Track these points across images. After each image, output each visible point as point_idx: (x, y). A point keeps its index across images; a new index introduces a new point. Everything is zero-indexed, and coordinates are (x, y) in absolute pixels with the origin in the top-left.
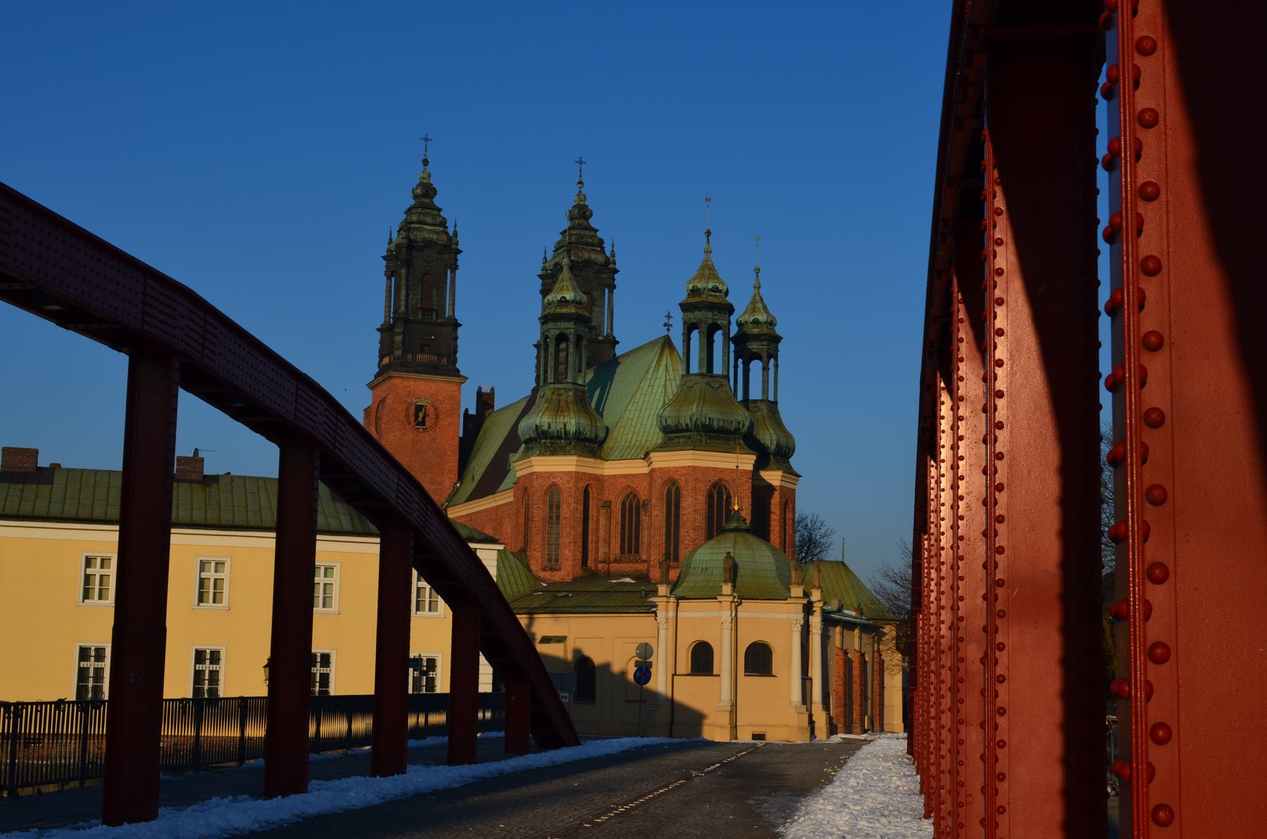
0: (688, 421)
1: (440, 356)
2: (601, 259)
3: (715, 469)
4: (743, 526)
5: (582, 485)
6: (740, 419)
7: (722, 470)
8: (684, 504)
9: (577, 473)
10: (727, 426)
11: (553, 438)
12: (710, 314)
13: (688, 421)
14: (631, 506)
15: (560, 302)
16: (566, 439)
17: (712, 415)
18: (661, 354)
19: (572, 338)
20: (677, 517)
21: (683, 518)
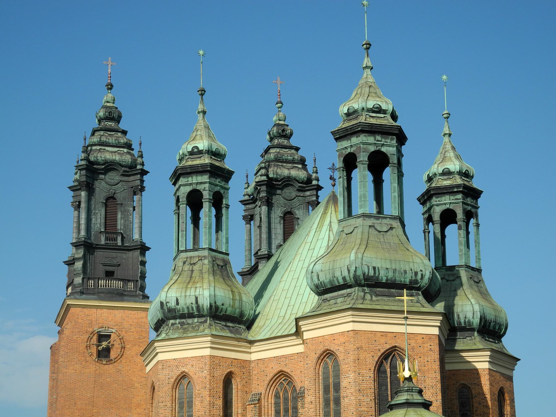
0: (345, 273)
1: (126, 281)
2: (301, 174)
3: (384, 334)
4: (417, 398)
5: (221, 374)
6: (417, 268)
7: (395, 335)
8: (344, 383)
9: (212, 357)
10: (400, 279)
11: (183, 316)
12: (371, 139)
13: (345, 273)
14: (286, 399)
15: (191, 153)
16: (200, 316)
17: (378, 264)
18: (325, 213)
19: (206, 195)
20: (337, 401)
21: (344, 402)
